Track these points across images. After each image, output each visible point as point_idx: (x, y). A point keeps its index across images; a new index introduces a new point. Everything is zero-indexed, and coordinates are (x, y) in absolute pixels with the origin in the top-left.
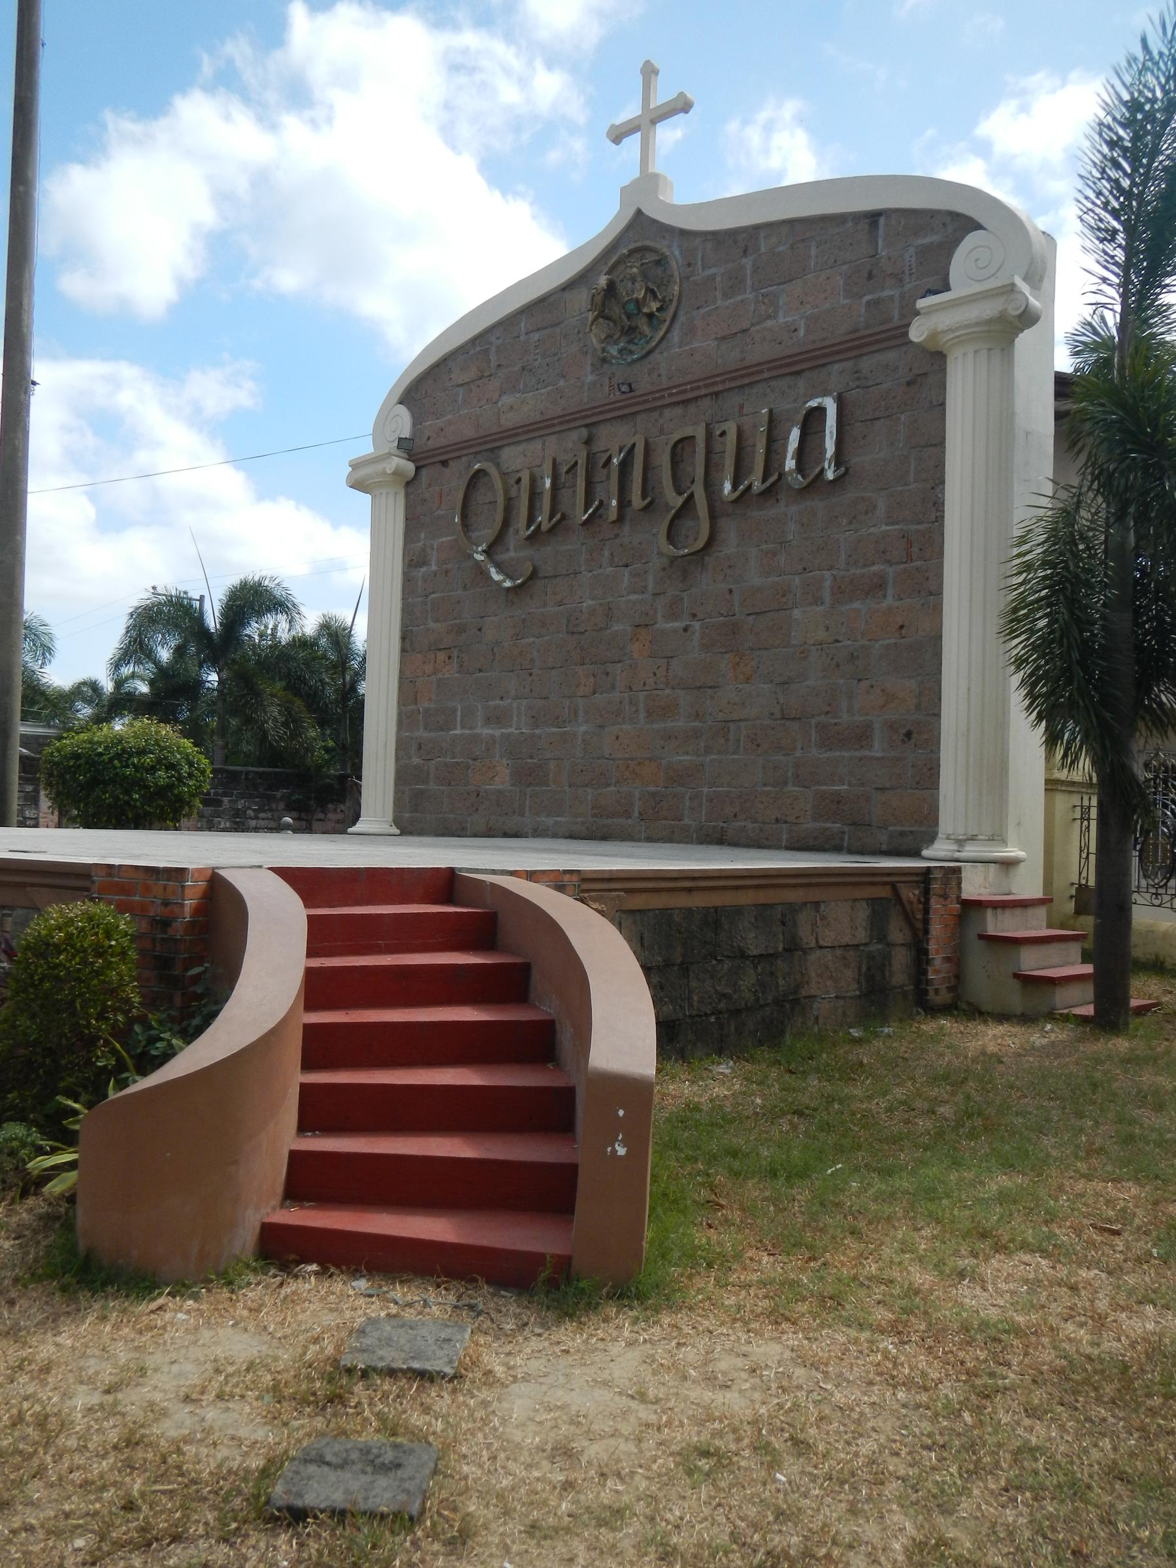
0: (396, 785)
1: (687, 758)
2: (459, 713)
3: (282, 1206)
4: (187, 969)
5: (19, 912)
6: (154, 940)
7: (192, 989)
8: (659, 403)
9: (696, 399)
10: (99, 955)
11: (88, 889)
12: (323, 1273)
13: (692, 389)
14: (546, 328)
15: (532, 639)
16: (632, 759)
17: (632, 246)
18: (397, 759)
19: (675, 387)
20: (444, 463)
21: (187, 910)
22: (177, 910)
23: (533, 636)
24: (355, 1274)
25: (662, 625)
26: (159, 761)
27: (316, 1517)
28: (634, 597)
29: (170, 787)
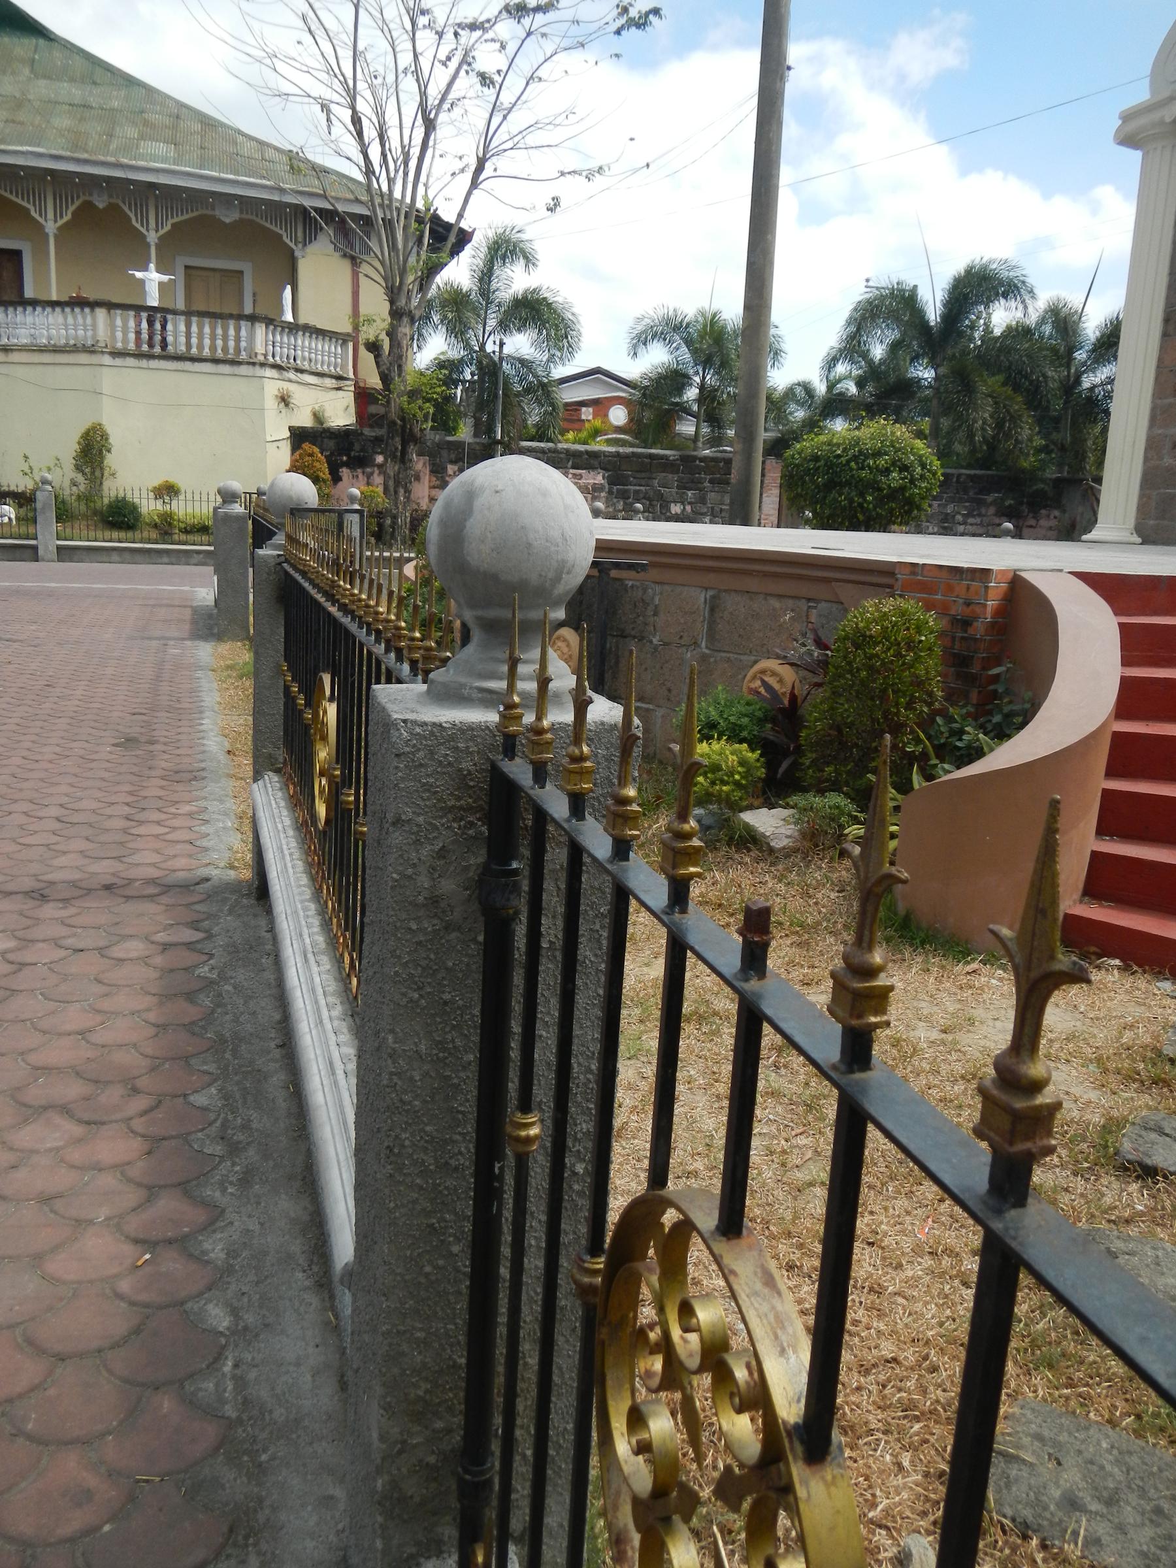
0: (1142, 487)
3: (1081, 902)
4: (984, 669)
5: (823, 605)
6: (953, 638)
7: (991, 687)
10: (909, 648)
11: (891, 587)
12: (1125, 969)
18: (1146, 459)
21: (989, 609)
22: (978, 609)
24: (1159, 975)
26: (894, 463)
27: (1165, 1177)
29: (903, 489)
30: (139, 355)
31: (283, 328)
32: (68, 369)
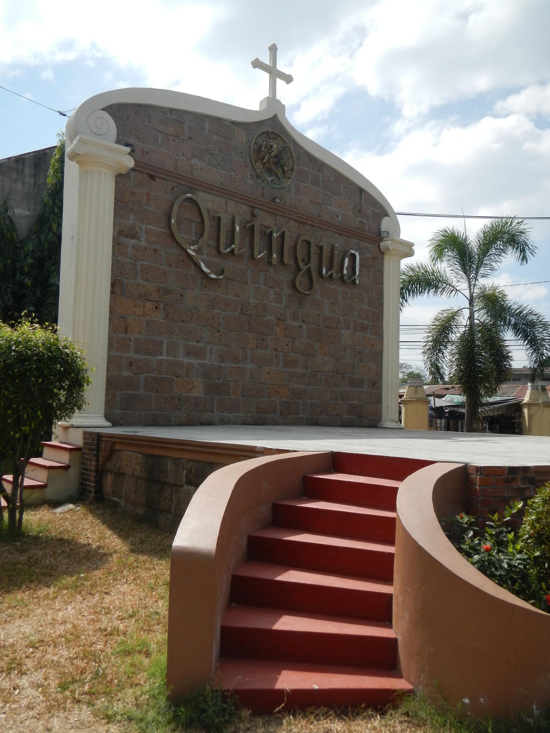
0: (107, 390)
1: (301, 386)
2: (165, 346)
8: (291, 217)
9: (304, 223)
13: (306, 219)
14: (221, 136)
15: (220, 311)
16: (275, 385)
17: (273, 130)
18: (108, 370)
19: (299, 214)
20: (152, 177)
23: (220, 309)
25: (289, 322)
28: (276, 304)
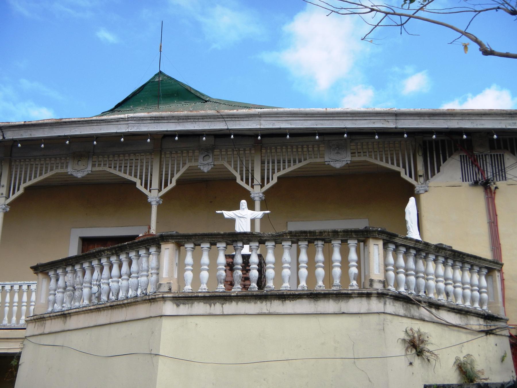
30: (210, 298)
31: (408, 248)
32: (124, 329)
